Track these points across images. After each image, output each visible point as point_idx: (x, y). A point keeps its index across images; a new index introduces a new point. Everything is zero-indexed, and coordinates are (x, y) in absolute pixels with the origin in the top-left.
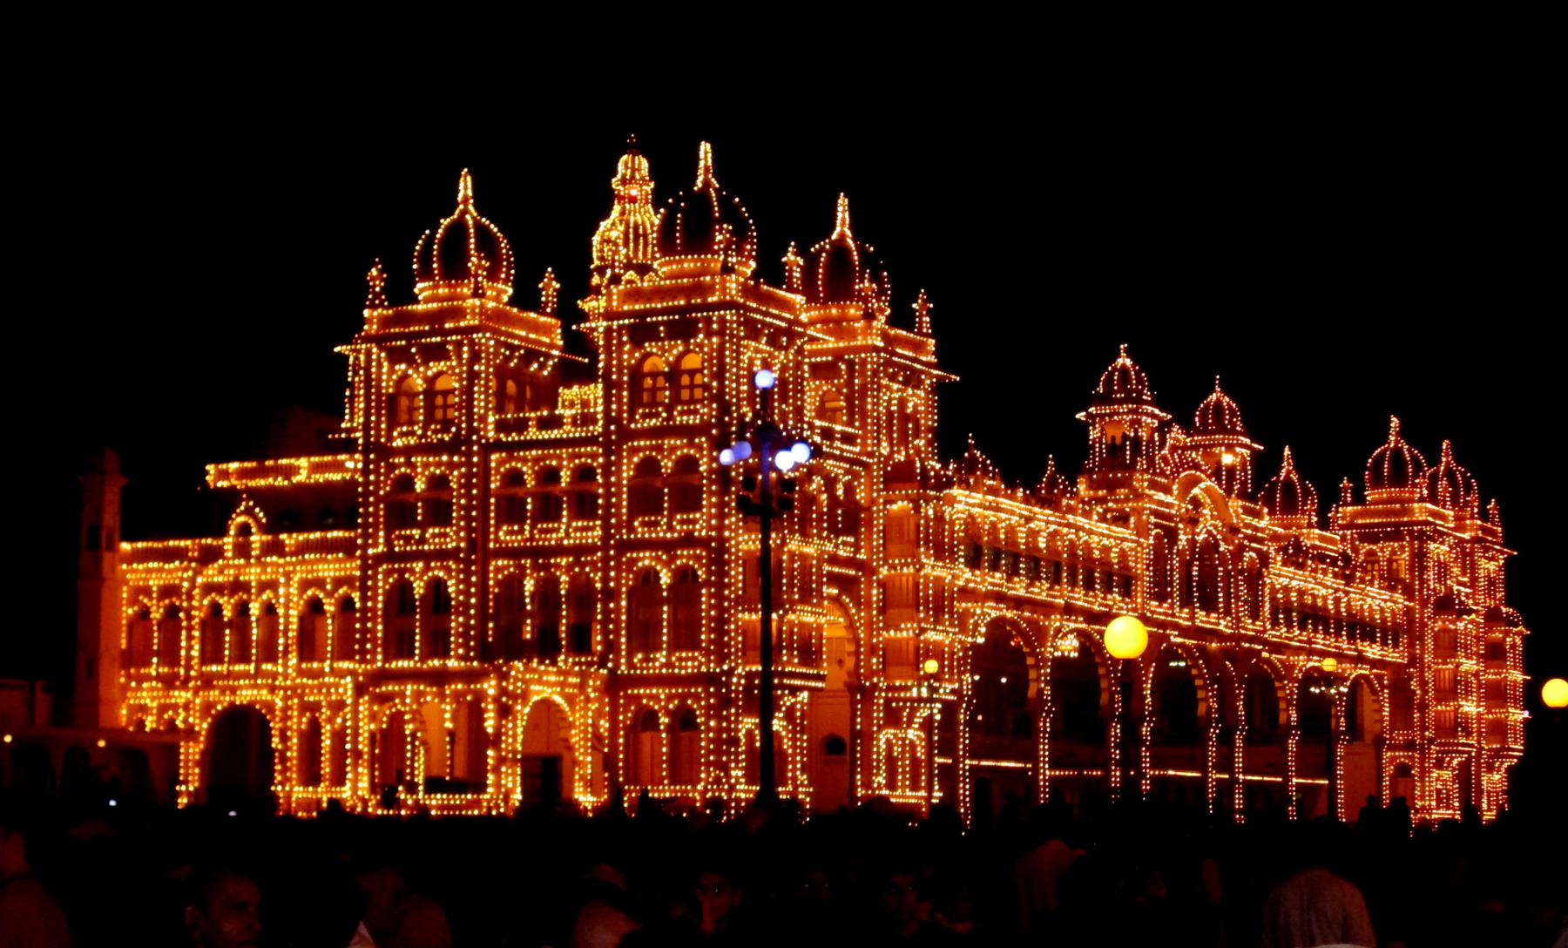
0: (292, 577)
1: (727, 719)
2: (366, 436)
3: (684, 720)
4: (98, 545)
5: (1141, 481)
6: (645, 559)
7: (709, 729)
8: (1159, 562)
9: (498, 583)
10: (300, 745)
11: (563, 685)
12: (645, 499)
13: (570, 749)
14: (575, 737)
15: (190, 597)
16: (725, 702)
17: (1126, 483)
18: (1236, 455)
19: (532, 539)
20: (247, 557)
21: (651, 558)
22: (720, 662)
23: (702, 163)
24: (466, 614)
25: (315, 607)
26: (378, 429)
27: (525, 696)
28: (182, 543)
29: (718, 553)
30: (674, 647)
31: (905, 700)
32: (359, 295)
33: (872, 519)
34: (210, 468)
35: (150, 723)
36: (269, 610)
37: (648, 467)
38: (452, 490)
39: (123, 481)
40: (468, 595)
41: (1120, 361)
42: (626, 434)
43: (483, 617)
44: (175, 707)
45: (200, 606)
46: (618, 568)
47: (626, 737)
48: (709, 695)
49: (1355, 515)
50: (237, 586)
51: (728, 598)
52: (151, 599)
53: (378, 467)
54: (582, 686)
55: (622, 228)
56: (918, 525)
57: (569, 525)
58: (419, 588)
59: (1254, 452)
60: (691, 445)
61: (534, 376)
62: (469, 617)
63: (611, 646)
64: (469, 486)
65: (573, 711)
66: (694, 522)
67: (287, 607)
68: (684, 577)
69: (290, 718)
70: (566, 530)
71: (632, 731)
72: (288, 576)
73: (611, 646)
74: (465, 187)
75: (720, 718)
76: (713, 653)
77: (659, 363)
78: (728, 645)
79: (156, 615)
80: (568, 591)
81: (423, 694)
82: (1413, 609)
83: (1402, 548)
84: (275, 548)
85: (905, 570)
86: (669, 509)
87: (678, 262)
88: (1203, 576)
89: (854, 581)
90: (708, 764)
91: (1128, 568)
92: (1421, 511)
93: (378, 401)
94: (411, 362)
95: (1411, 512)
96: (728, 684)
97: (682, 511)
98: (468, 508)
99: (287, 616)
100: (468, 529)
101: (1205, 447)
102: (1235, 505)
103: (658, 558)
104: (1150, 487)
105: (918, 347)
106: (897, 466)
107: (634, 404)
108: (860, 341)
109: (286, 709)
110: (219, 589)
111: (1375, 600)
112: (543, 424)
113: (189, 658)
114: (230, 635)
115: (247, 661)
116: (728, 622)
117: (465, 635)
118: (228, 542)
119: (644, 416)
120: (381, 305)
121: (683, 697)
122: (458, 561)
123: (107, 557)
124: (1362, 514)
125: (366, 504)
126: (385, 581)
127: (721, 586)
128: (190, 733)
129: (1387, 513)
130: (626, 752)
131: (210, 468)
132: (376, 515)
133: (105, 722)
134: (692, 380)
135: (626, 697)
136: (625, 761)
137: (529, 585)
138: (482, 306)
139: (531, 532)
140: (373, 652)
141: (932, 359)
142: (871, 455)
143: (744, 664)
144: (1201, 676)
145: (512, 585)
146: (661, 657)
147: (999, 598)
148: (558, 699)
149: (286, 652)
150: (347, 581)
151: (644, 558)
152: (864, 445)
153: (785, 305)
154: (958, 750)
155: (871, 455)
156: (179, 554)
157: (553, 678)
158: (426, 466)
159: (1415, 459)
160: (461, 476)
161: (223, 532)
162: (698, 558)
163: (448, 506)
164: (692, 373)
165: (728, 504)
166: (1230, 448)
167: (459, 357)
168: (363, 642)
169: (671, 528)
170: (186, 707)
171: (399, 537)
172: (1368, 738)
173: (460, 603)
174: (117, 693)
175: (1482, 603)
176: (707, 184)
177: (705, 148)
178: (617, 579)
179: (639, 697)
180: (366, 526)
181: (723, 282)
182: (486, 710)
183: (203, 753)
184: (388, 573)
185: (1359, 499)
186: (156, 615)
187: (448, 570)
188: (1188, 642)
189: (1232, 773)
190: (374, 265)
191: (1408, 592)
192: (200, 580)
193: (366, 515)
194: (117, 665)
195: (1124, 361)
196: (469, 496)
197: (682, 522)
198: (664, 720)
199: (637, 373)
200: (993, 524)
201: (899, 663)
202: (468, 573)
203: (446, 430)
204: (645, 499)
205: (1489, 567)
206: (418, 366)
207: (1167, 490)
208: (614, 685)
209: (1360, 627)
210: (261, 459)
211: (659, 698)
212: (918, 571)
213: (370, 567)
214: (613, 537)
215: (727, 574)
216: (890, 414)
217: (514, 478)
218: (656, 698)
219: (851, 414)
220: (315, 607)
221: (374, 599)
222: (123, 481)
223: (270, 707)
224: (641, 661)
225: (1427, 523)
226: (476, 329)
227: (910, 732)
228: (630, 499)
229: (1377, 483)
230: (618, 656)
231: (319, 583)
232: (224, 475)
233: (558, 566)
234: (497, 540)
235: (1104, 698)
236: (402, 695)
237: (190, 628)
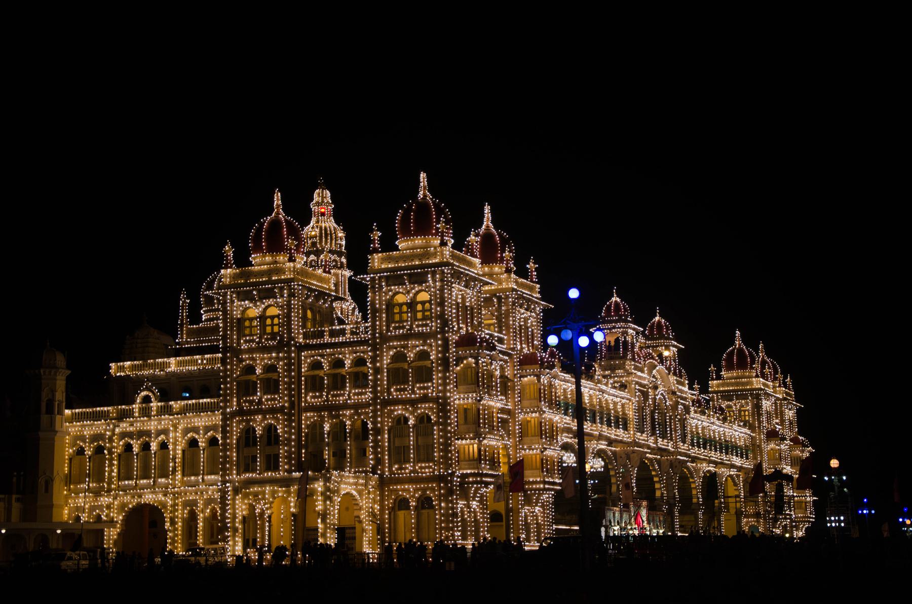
0: (177, 427)
1: (451, 501)
2: (225, 343)
3: (425, 503)
4: (51, 410)
5: (629, 365)
6: (399, 410)
7: (441, 508)
8: (640, 410)
9: (308, 427)
10: (183, 527)
11: (356, 484)
12: (398, 376)
13: (360, 522)
14: (363, 515)
15: (111, 440)
16: (451, 492)
17: (622, 366)
18: (669, 350)
19: (327, 400)
20: (149, 416)
21: (403, 410)
22: (446, 469)
23: (422, 184)
24: (289, 445)
25: (193, 443)
26: (232, 340)
27: (338, 491)
28: (106, 409)
29: (443, 406)
30: (418, 460)
31: (535, 490)
33: (514, 386)
34: (113, 365)
35: (84, 517)
36: (164, 446)
37: (399, 357)
38: (279, 373)
39: (68, 372)
40: (290, 434)
41: (614, 299)
42: (385, 339)
43: (299, 447)
44: (100, 507)
45: (118, 446)
46: (381, 416)
47: (390, 514)
48: (440, 488)
49: (718, 386)
50: (141, 434)
51: (450, 432)
52: (85, 442)
53: (232, 361)
54: (366, 485)
55: (318, 230)
56: (540, 389)
57: (350, 392)
58: (259, 431)
59: (679, 350)
61: (320, 307)
62: (291, 447)
63: (379, 461)
64: (289, 371)
65: (362, 499)
66: (428, 388)
67: (175, 444)
68: (423, 420)
69: (177, 510)
70: (350, 394)
71: (392, 510)
72: (175, 427)
73: (379, 461)
74: (277, 199)
75: (447, 502)
76: (442, 463)
78: (451, 459)
79: (88, 452)
80: (351, 429)
81: (277, 492)
82: (755, 437)
83: (747, 404)
85: (534, 415)
86: (412, 381)
87: (412, 240)
88: (657, 419)
90: (441, 528)
91: (626, 415)
92: (757, 383)
93: (232, 322)
94: (252, 299)
95: (751, 383)
96: (451, 482)
97: (420, 382)
98: (290, 384)
99: (175, 450)
100: (290, 396)
101: (653, 347)
102: (672, 379)
103: (407, 409)
104: (635, 369)
105: (531, 289)
106: (526, 356)
107: (389, 321)
108: (504, 286)
109: (174, 505)
110: (130, 435)
111: (738, 433)
112: (333, 334)
113: (110, 477)
114: (144, 461)
115: (148, 478)
116: (450, 445)
117: (289, 457)
118: (136, 407)
119: (395, 328)
120: (231, 267)
121: (424, 490)
122: (283, 414)
123: (58, 417)
124: (723, 385)
125: (225, 383)
126: (237, 427)
127: (446, 424)
128: (111, 522)
129: (737, 384)
130: (390, 523)
131: (113, 365)
132: (231, 389)
133: (55, 519)
134: (400, 309)
135: (389, 490)
136: (389, 528)
137: (327, 427)
138: (294, 267)
139: (327, 396)
140: (231, 469)
141: (539, 296)
142: (513, 349)
143: (459, 469)
144: (657, 476)
145: (316, 427)
146: (409, 467)
148: (355, 493)
149: (174, 470)
150: (214, 428)
151: (397, 410)
152: (509, 344)
153: (470, 264)
155: (513, 349)
157: (352, 481)
158: (262, 359)
159: (750, 353)
160: (285, 364)
161: (133, 402)
162: (431, 409)
163: (277, 382)
164: (423, 303)
165: (449, 378)
166: (667, 348)
167: (282, 296)
168: (224, 463)
169: (414, 392)
170: (109, 507)
171: (245, 402)
173: (286, 439)
175: (788, 434)
176: (425, 196)
177: (423, 176)
178: (382, 423)
179: (397, 490)
180: (225, 395)
181: (442, 252)
182: (317, 500)
183: (119, 534)
184: (239, 422)
185: (719, 377)
186: (88, 452)
187: (277, 419)
190: (227, 244)
191: (752, 428)
192: (117, 430)
193: (226, 389)
194: (63, 484)
195: (615, 299)
196: (290, 377)
197: (420, 388)
199: (390, 305)
200: (564, 389)
202: (290, 421)
203: (273, 339)
204: (398, 376)
205: (790, 414)
206: (256, 301)
207: (642, 372)
208: (383, 483)
209: (728, 447)
210: (145, 359)
211: (410, 492)
212: (541, 415)
213: (228, 419)
214: (379, 398)
215: (449, 418)
216: (520, 326)
217: (317, 365)
218: (408, 491)
219: (500, 327)
220: (193, 443)
221: (231, 438)
222: (68, 372)
223: (164, 505)
224: (397, 469)
225: (761, 389)
226: (292, 280)
227: (537, 508)
228: (388, 376)
229: (730, 368)
230: (384, 466)
231: (196, 430)
232: (122, 369)
233: (345, 415)
234: (306, 401)
235: (614, 488)
236: (264, 493)
237: (111, 460)
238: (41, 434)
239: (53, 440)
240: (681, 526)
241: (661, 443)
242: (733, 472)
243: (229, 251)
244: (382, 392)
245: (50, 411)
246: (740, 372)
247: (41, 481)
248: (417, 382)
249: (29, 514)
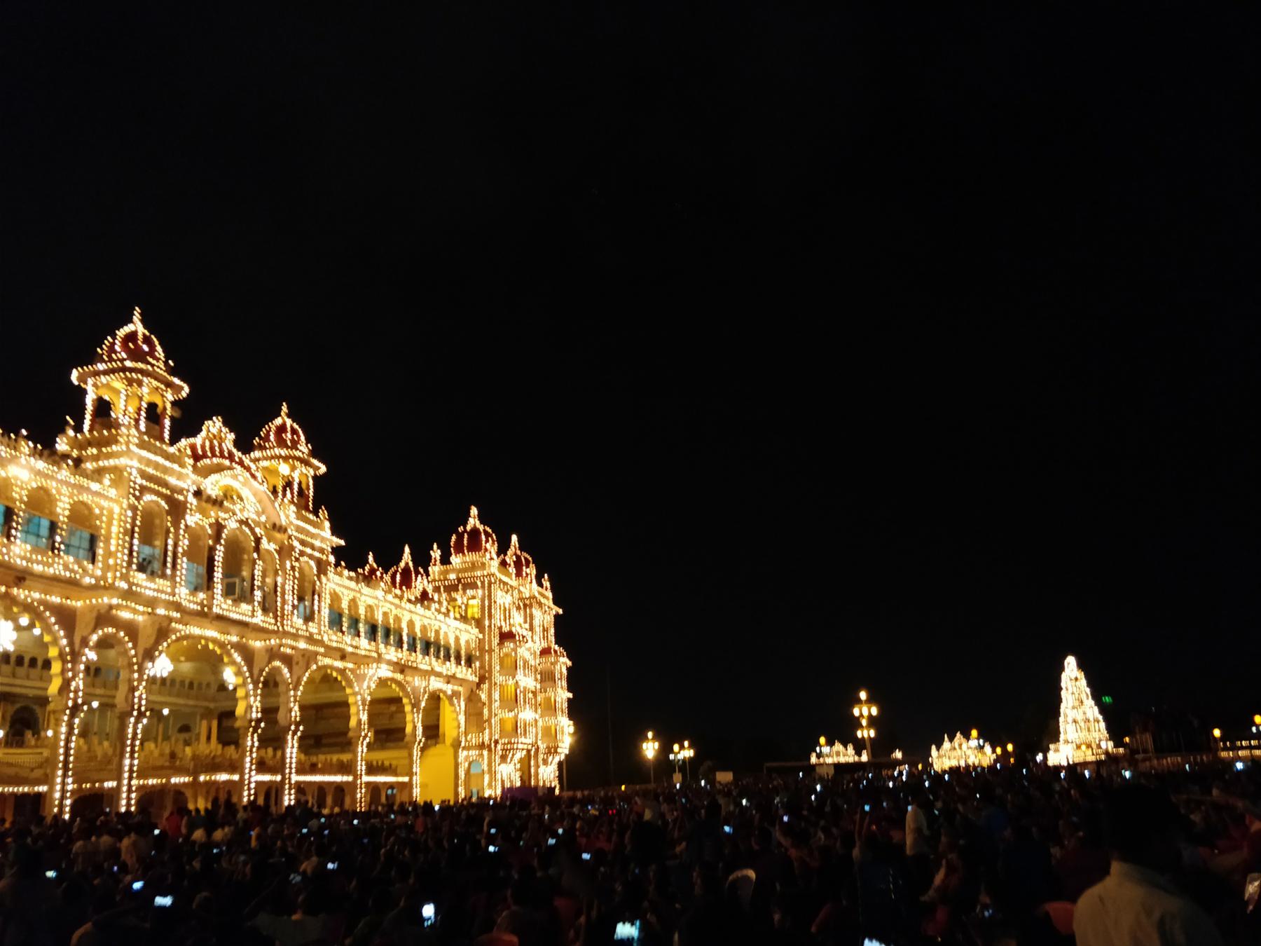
172: (449, 741)
175: (538, 645)
209: (430, 646)
229: (459, 549)
242: (436, 684)
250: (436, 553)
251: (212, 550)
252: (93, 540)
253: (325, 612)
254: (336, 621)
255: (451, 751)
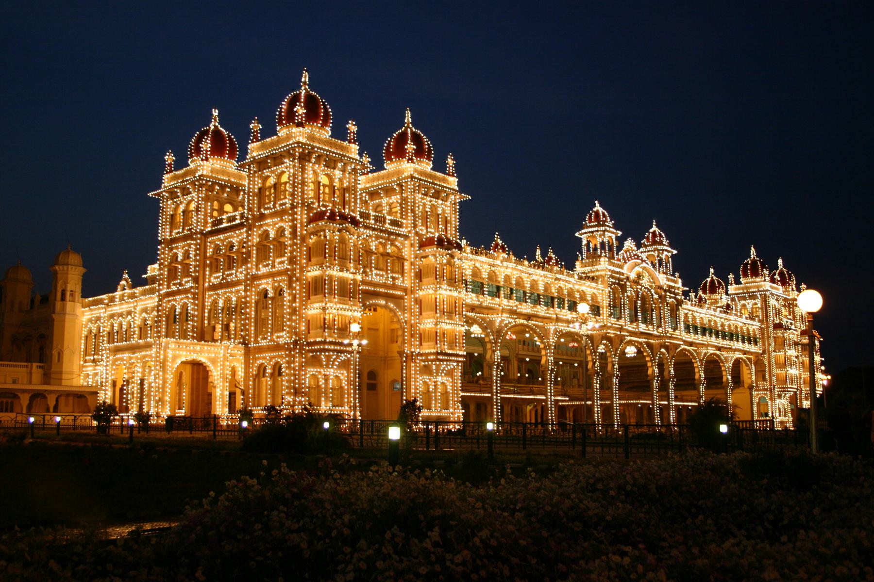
24: (193, 320)
32: (160, 169)
47: (254, 380)
49: (736, 289)
60: (282, 220)
77: (272, 181)
84: (132, 296)
89: (401, 298)
118: (118, 294)
123: (69, 305)
130: (254, 388)
136: (254, 395)
144: (648, 356)
147: (512, 312)
154: (492, 389)
156: (101, 302)
161: (115, 290)
169: (273, 266)
172: (746, 386)
174: (76, 369)
185: (738, 282)
188: (640, 340)
189: (668, 401)
195: (598, 207)
198: (269, 371)
201: (428, 340)
202: (194, 298)
227: (439, 379)
229: (745, 275)
234: (210, 281)
235: (590, 365)
238: (54, 316)
239: (64, 321)
240: (676, 397)
241: (642, 327)
242: (738, 355)
243: (169, 158)
244: (251, 269)
245: (63, 299)
246: (754, 279)
247: (55, 352)
248: (277, 257)
249: (47, 378)
250: (731, 276)
251: (636, 303)
252: (598, 308)
253: (682, 325)
254: (687, 328)
255: (748, 391)
